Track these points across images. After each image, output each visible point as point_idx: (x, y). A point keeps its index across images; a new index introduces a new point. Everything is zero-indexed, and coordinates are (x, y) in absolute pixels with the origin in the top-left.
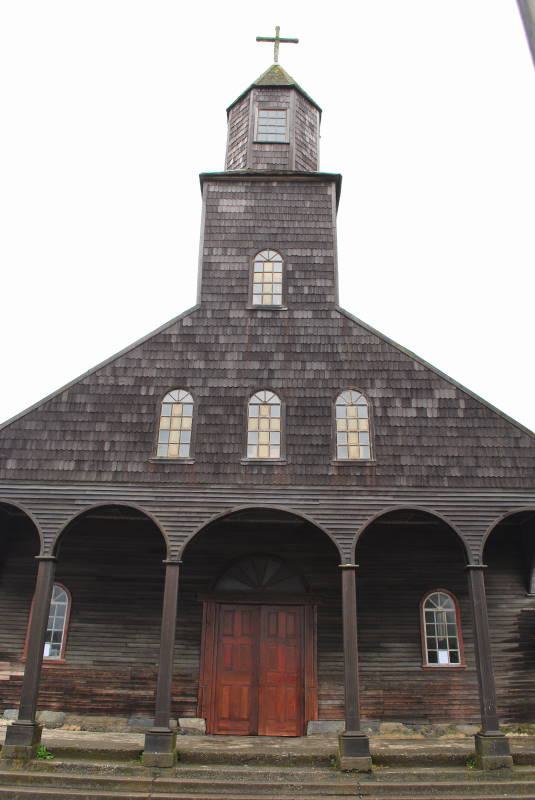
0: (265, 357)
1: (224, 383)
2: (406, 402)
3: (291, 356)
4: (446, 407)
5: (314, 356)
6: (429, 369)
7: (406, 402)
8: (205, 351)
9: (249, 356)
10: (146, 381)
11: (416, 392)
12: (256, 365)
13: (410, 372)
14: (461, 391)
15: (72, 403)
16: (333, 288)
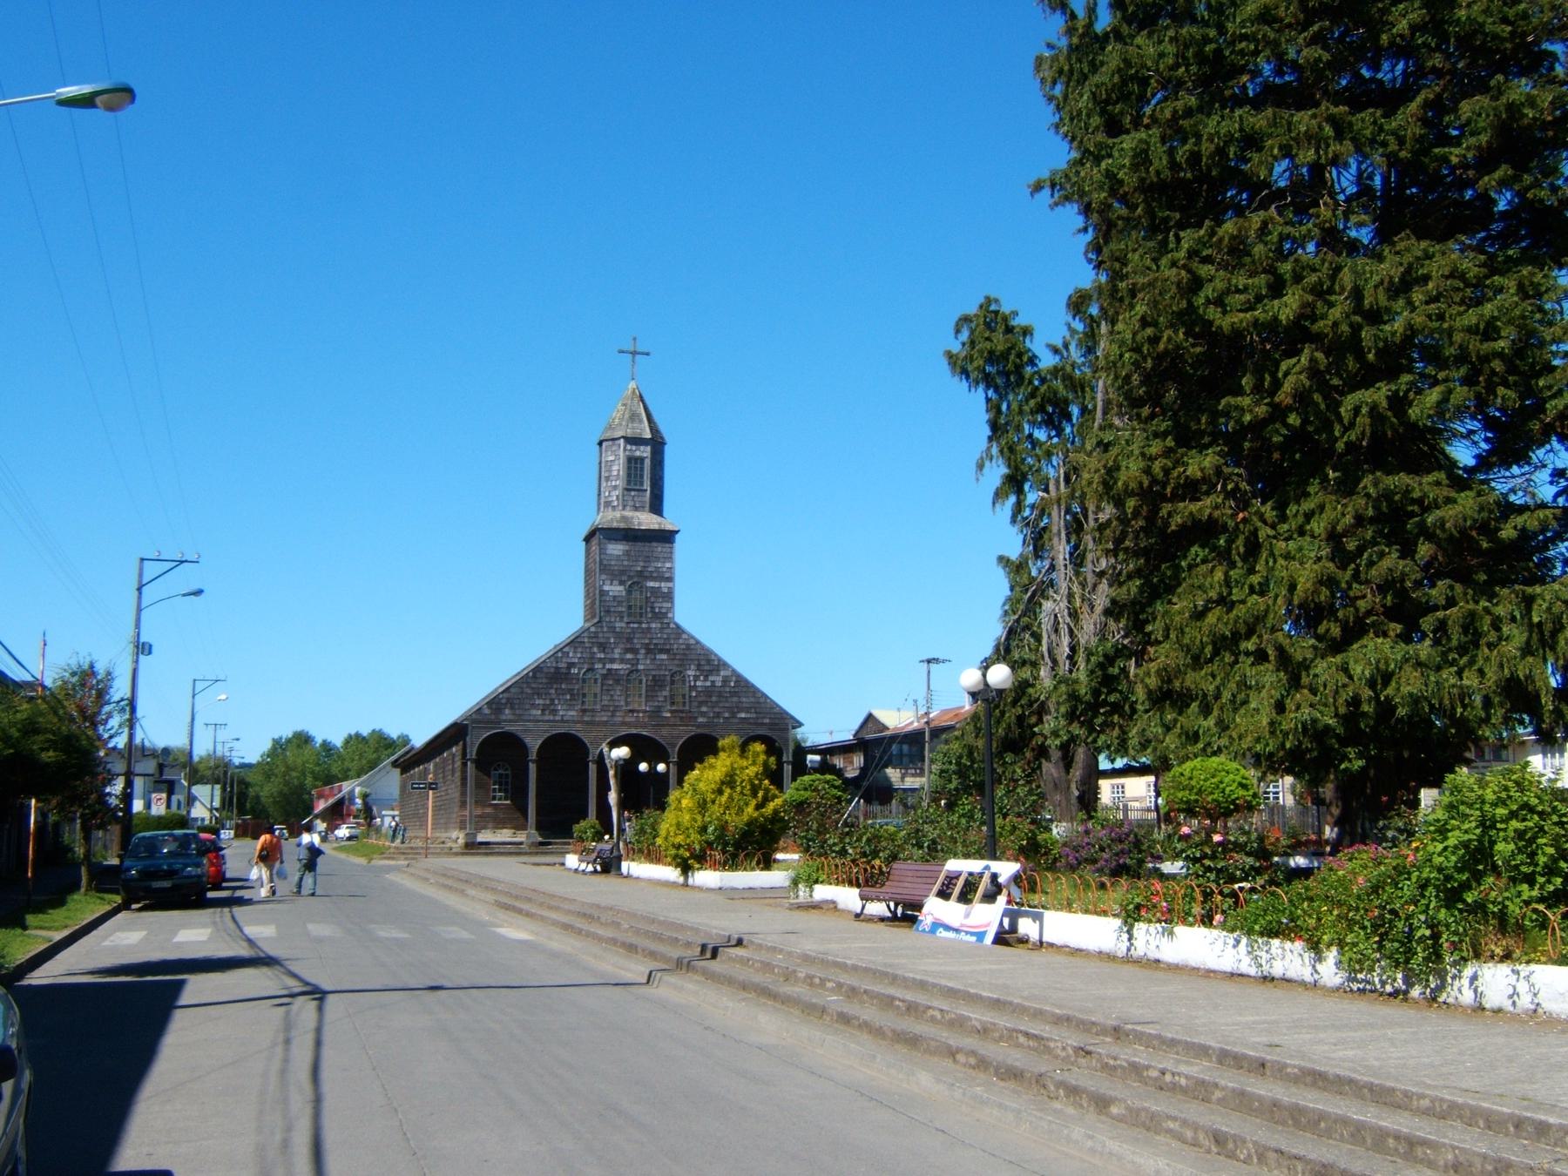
0: (634, 651)
1: (615, 666)
2: (706, 679)
3: (649, 651)
4: (725, 681)
5: (662, 651)
6: (719, 660)
7: (706, 679)
8: (603, 647)
9: (627, 651)
10: (571, 665)
11: (711, 672)
12: (629, 656)
13: (709, 661)
14: (734, 671)
15: (534, 677)
16: (671, 609)
